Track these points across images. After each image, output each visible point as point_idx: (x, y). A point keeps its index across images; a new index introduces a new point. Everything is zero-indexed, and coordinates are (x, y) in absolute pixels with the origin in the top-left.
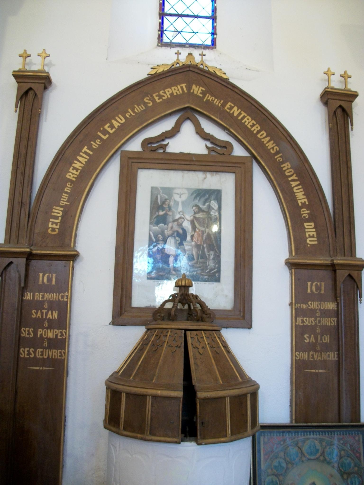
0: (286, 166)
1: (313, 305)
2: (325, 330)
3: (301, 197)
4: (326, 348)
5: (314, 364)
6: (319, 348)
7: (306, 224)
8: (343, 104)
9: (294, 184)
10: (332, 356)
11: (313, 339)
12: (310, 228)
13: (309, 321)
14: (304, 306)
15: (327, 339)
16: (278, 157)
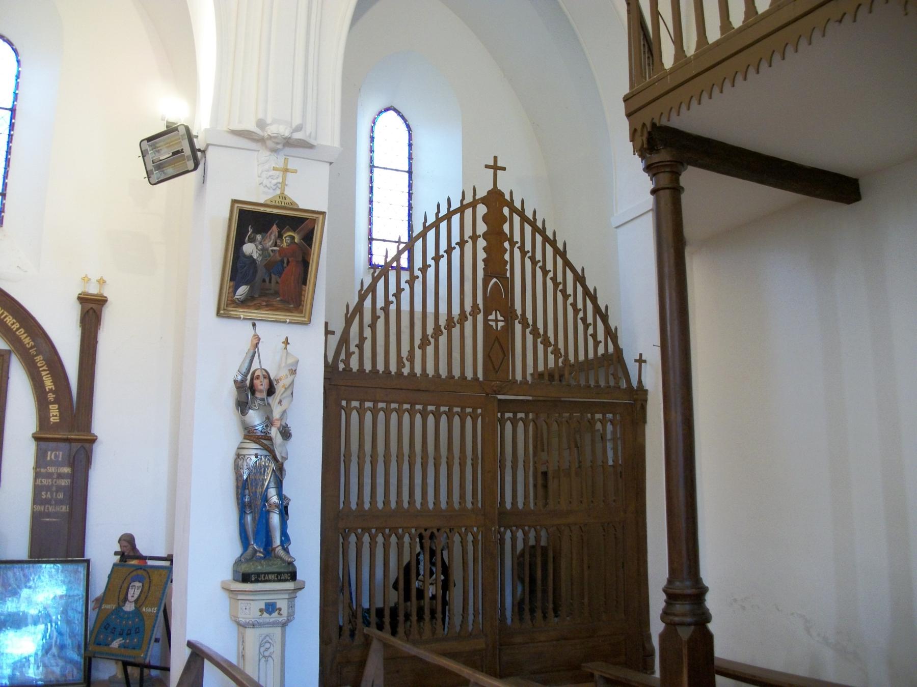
0: (39, 359)
1: (51, 470)
2: (59, 489)
3: (49, 384)
4: (60, 502)
5: (48, 515)
6: (53, 502)
7: (51, 406)
8: (94, 306)
9: (43, 373)
10: (65, 509)
11: (49, 495)
12: (54, 410)
13: (45, 482)
14: (43, 470)
15: (61, 496)
16: (33, 351)
